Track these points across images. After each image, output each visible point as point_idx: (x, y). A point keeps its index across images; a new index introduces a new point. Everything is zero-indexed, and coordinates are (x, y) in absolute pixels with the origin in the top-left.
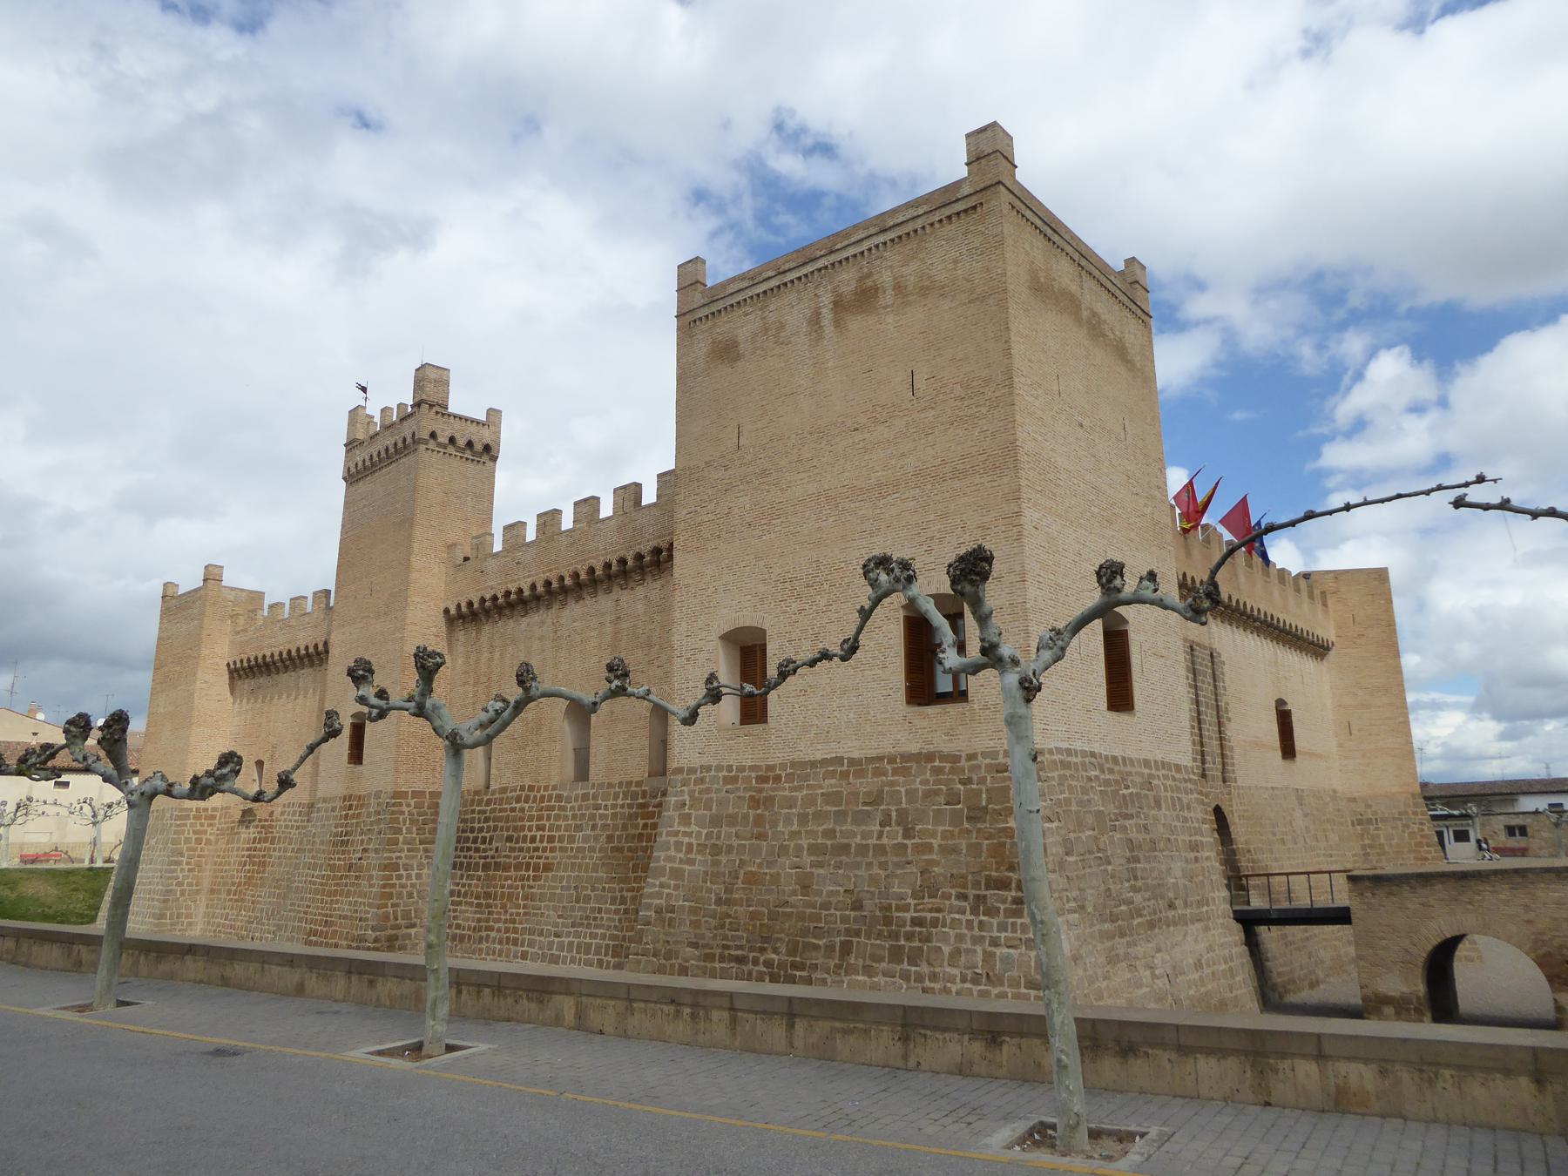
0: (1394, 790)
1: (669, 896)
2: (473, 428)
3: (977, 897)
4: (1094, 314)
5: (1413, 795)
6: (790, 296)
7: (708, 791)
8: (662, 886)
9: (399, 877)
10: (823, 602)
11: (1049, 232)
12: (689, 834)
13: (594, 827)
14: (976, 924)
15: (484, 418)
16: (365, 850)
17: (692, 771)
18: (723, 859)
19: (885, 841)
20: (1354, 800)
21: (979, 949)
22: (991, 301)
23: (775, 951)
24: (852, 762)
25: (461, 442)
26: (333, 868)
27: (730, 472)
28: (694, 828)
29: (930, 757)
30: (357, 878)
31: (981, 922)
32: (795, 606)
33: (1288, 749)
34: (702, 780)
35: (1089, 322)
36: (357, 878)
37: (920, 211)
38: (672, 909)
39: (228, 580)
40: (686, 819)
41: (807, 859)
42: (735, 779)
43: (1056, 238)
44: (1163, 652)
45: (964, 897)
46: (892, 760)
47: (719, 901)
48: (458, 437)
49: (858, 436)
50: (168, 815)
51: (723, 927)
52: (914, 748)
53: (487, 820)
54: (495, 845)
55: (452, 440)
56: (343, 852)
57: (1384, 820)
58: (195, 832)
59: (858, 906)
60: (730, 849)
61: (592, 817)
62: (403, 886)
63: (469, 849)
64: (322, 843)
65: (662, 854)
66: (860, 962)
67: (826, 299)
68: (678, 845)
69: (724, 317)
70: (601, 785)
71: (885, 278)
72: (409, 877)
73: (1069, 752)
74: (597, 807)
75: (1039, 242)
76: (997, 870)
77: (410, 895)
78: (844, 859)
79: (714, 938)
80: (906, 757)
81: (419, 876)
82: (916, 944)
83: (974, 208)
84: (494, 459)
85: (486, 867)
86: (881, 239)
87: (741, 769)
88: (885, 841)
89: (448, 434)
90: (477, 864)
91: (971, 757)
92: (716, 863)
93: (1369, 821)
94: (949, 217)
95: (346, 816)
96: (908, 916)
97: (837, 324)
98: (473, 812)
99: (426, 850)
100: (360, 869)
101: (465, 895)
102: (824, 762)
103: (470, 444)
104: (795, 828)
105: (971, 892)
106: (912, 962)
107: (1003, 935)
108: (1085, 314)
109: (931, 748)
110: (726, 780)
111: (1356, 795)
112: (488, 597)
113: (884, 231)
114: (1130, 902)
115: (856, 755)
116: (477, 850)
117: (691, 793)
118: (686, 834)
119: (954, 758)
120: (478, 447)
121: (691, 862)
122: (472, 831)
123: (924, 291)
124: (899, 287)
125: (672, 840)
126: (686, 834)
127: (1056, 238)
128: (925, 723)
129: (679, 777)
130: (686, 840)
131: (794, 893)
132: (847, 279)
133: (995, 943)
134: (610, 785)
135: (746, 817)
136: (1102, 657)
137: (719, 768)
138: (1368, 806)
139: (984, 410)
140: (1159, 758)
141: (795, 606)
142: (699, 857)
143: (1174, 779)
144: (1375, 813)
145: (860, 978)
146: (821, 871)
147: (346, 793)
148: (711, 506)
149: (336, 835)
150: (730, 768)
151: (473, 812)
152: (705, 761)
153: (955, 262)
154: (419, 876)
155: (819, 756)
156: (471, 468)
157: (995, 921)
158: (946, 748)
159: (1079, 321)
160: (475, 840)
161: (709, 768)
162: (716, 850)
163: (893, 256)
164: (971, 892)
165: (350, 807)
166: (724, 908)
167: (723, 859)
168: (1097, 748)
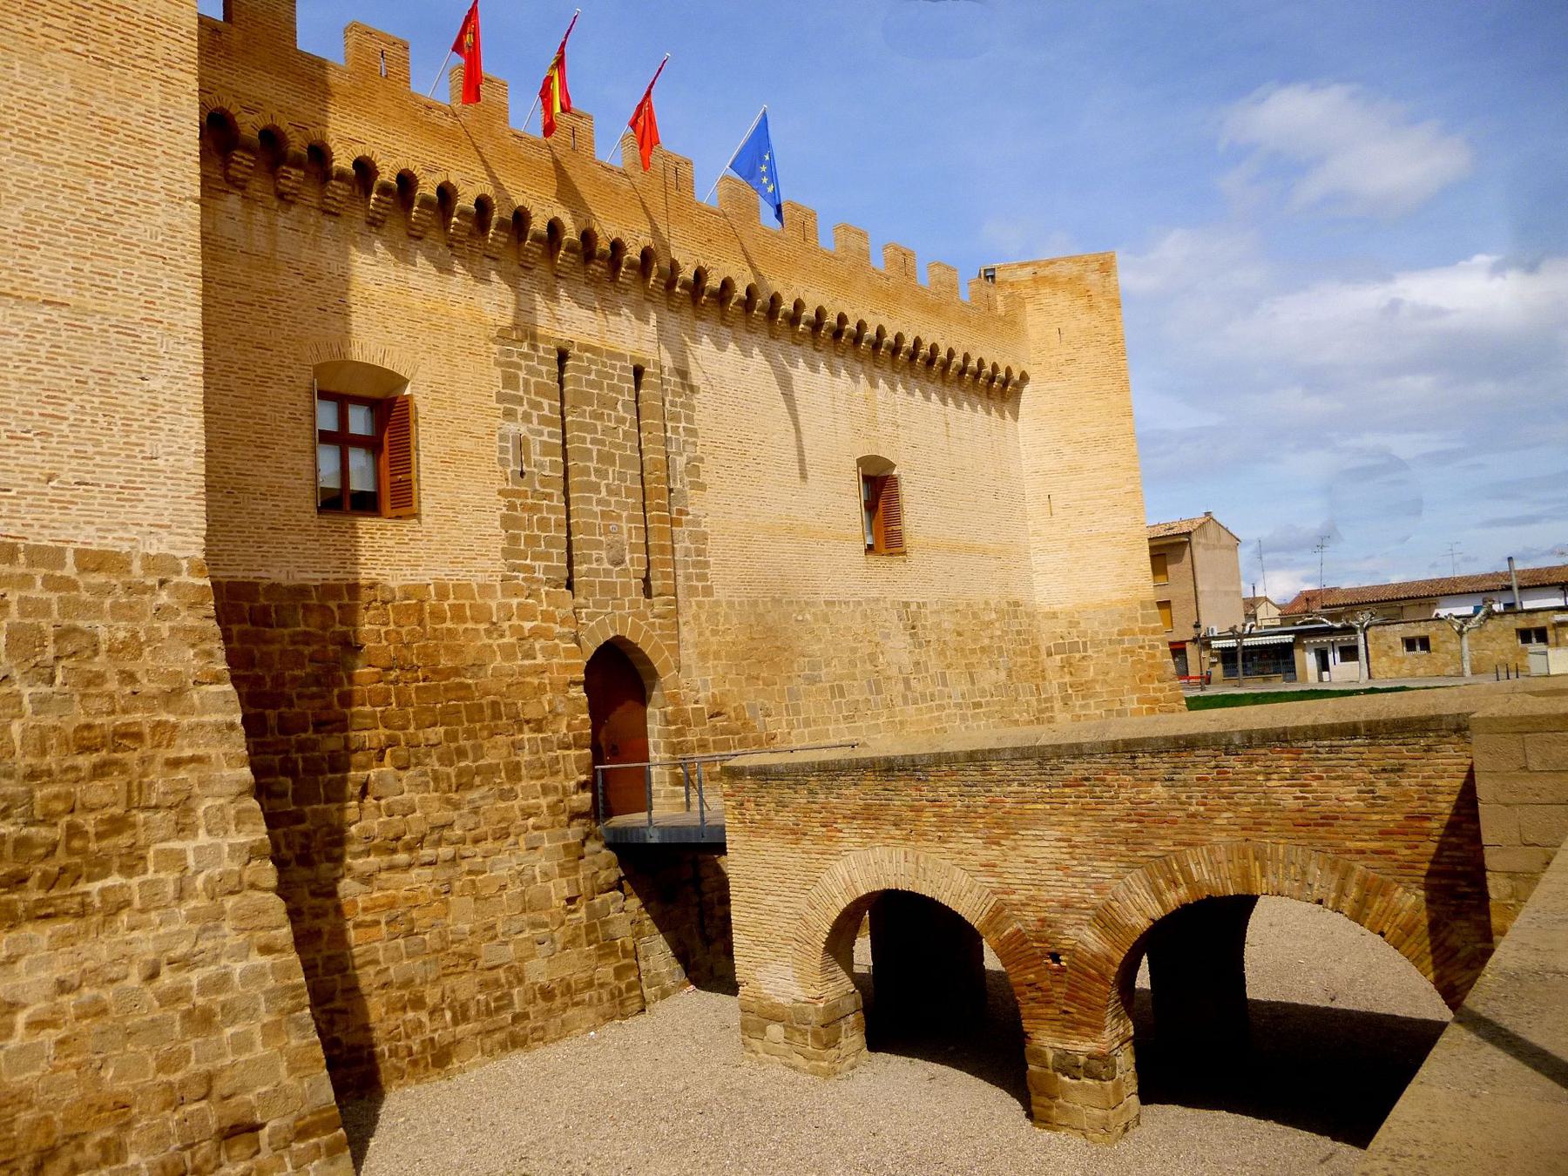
0: (1115, 596)
5: (1143, 605)
20: (1054, 615)
44: (68, 295)
57: (1097, 644)
93: (1073, 647)
111: (1057, 607)
138: (1073, 624)
144: (1085, 634)
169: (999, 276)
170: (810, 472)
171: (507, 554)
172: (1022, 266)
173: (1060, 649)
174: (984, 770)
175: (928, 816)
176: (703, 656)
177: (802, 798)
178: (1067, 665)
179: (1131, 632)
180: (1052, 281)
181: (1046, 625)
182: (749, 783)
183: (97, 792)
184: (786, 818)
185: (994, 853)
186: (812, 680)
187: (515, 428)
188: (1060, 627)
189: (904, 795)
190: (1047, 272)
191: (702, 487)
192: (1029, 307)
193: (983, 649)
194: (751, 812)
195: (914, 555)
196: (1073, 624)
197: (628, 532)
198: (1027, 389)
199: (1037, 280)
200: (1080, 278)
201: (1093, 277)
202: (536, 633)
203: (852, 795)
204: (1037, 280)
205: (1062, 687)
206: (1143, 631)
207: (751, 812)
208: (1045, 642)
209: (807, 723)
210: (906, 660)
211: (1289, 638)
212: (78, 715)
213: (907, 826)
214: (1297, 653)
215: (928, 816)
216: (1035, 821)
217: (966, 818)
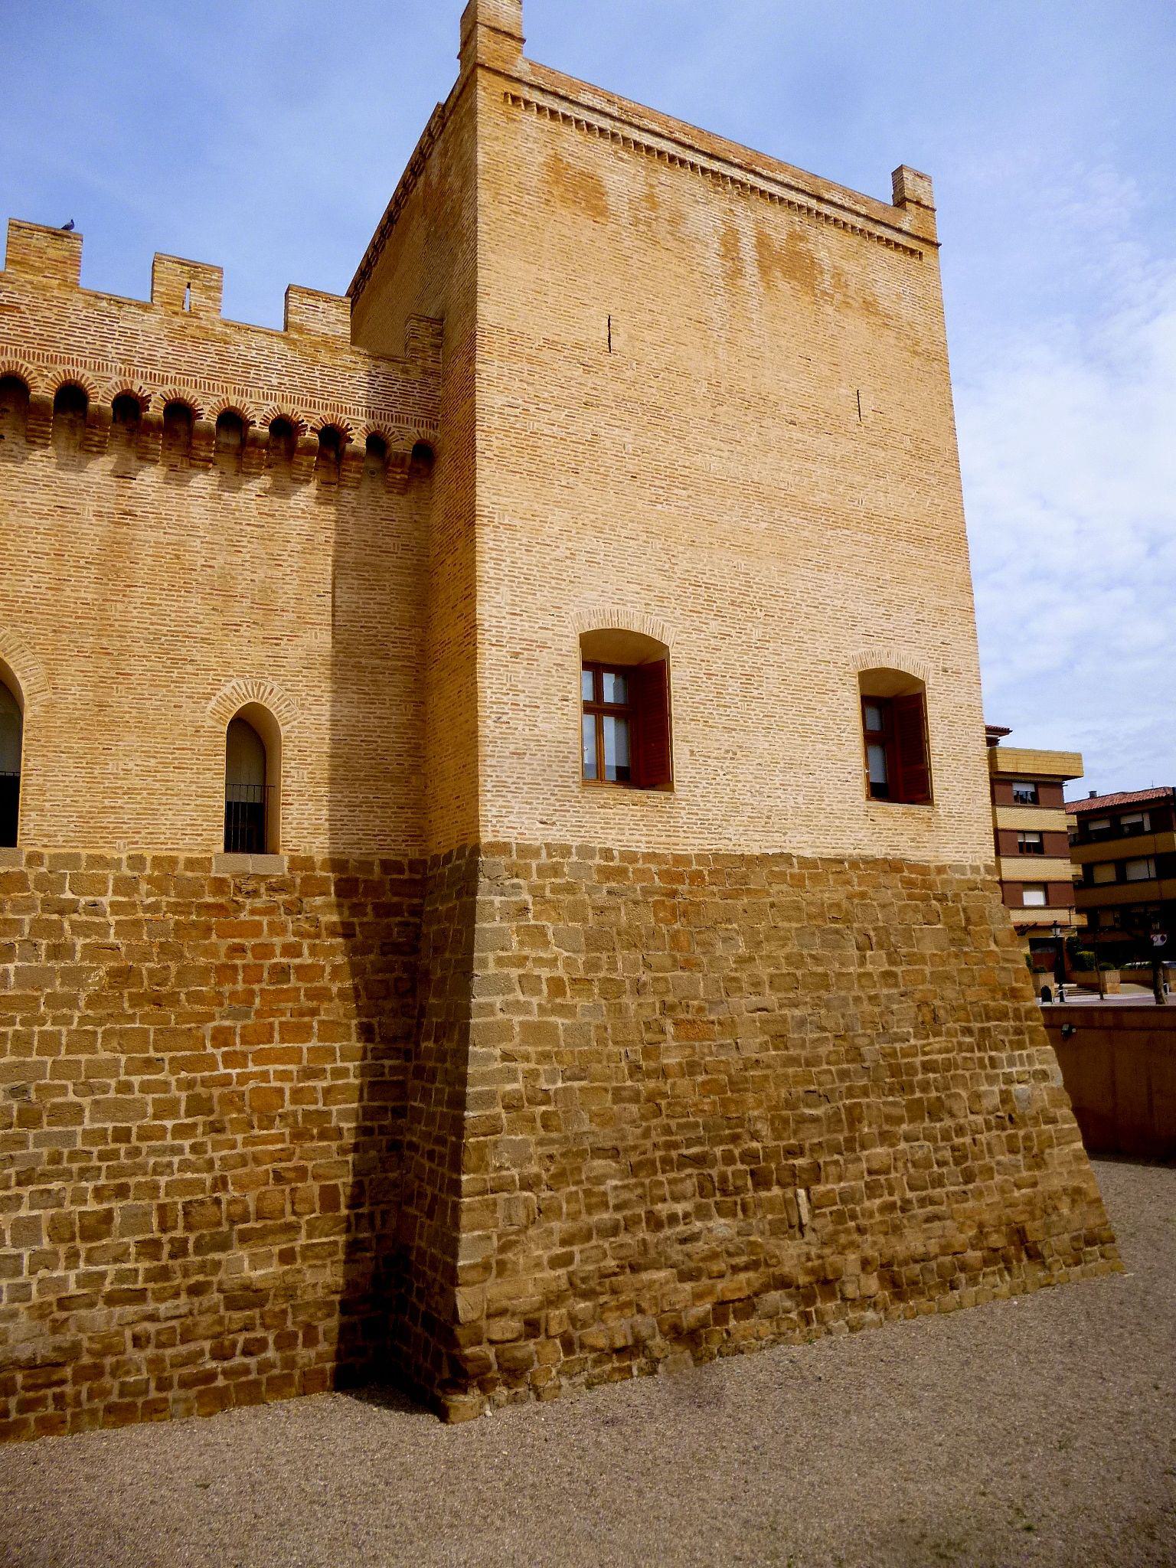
1: (532, 1075)
3: (982, 1030)
7: (570, 889)
10: (757, 634)
12: (552, 963)
14: (987, 1061)
17: (526, 851)
18: (628, 1001)
19: (869, 968)
21: (996, 1089)
23: (755, 1136)
24: (804, 862)
31: (991, 1058)
42: (622, 872)
45: (968, 1031)
46: (854, 864)
47: (635, 1069)
49: (796, 434)
51: (658, 1112)
52: (878, 851)
59: (855, 1054)
60: (639, 989)
65: (498, 1001)
66: (875, 1130)
76: (994, 999)
79: (646, 1135)
80: (871, 862)
82: (934, 1094)
87: (630, 857)
91: (941, 870)
92: (619, 1010)
96: (918, 1060)
102: (763, 859)
104: (743, 950)
106: (934, 1116)
107: (1014, 1070)
110: (607, 874)
115: (808, 853)
117: (537, 892)
118: (539, 961)
119: (923, 870)
121: (566, 1010)
125: (515, 973)
126: (539, 961)
128: (890, 824)
130: (545, 973)
131: (764, 1047)
133: (1009, 1080)
135: (653, 934)
142: (581, 1002)
145: (879, 1150)
146: (797, 1012)
150: (607, 854)
155: (757, 852)
157: (1004, 1055)
158: (914, 855)
161: (565, 851)
162: (612, 989)
166: (651, 1084)
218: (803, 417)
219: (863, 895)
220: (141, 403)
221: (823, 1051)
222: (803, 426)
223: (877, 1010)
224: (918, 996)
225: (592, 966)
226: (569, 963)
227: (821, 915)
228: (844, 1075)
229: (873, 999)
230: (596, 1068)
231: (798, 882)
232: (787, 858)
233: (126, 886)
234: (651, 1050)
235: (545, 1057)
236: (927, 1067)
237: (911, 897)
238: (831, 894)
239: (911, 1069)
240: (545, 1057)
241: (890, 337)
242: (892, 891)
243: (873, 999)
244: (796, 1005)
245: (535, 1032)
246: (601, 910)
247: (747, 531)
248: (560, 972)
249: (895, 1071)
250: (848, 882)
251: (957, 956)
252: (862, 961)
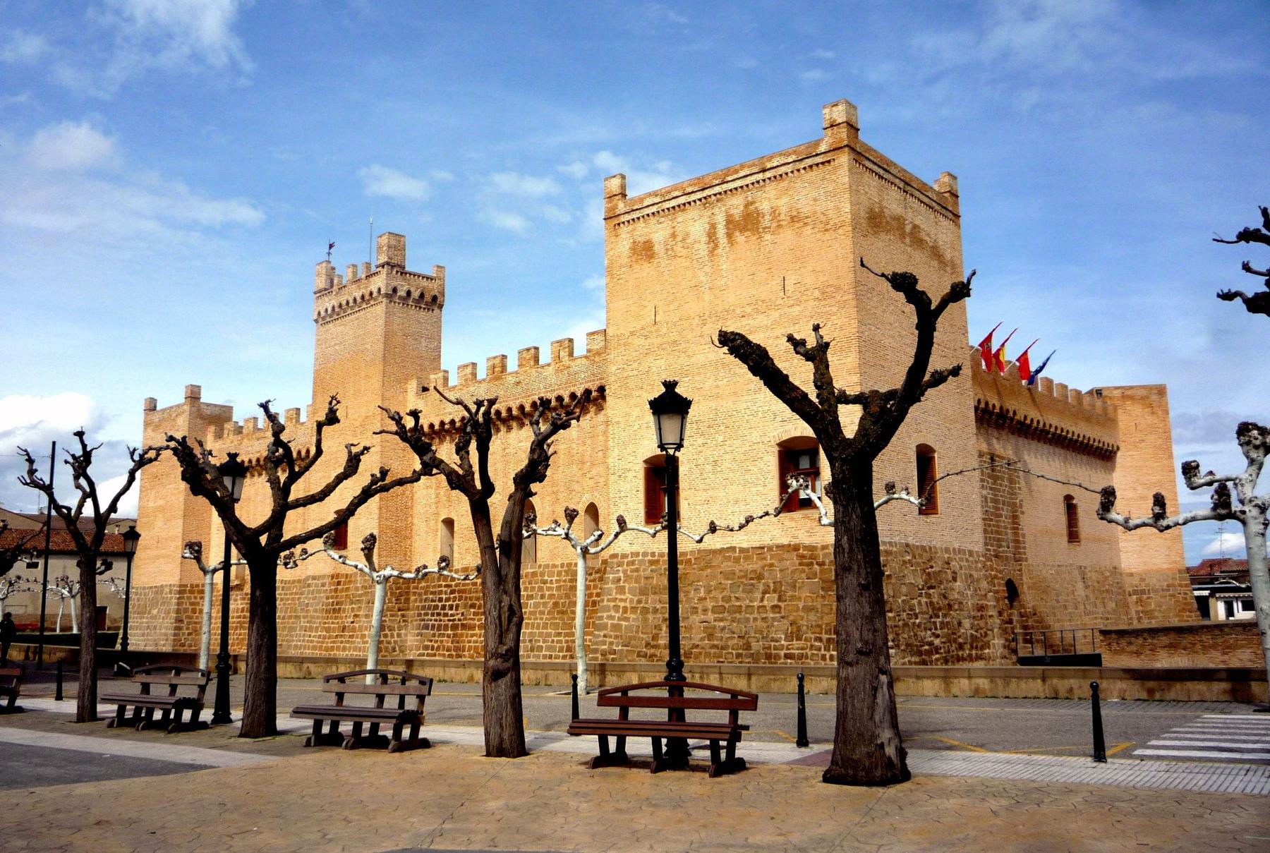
0: (1165, 566)
1: (611, 643)
2: (424, 283)
4: (915, 227)
5: (1180, 571)
6: (692, 212)
7: (637, 570)
8: (605, 636)
9: (386, 636)
10: (721, 438)
11: (882, 172)
12: (625, 600)
13: (543, 597)
15: (431, 272)
16: (356, 616)
17: (625, 556)
18: (650, 617)
19: (765, 603)
20: (1131, 575)
22: (841, 231)
24: (742, 550)
25: (416, 294)
26: (328, 630)
27: (649, 341)
28: (628, 596)
29: (796, 548)
30: (351, 637)
32: (700, 441)
33: (1073, 536)
34: (633, 563)
35: (911, 233)
36: (351, 637)
37: (790, 160)
38: (614, 652)
39: (205, 398)
40: (621, 590)
41: (710, 616)
42: (658, 561)
43: (886, 176)
45: (820, 640)
46: (770, 548)
47: (648, 645)
48: (412, 290)
50: (167, 590)
52: (785, 541)
53: (452, 592)
54: (460, 611)
55: (409, 293)
56: (336, 618)
57: (1156, 591)
58: (192, 604)
59: (748, 647)
61: (541, 589)
62: (389, 643)
63: (439, 614)
64: (316, 611)
65: (605, 615)
67: (720, 219)
68: (616, 608)
69: (641, 224)
70: (547, 566)
71: (765, 206)
72: (392, 636)
73: (890, 543)
74: (545, 582)
75: (875, 181)
77: (394, 650)
78: (738, 616)
81: (399, 635)
83: (829, 162)
84: (441, 307)
85: (454, 627)
86: (760, 176)
88: (765, 603)
89: (406, 288)
90: (446, 626)
92: (646, 620)
93: (1143, 592)
94: (811, 167)
95: (336, 590)
96: (782, 653)
97: (729, 235)
98: (440, 586)
99: (403, 616)
100: (354, 630)
101: (438, 648)
102: (722, 551)
103: (422, 296)
104: (702, 594)
105: (825, 637)
108: (908, 228)
109: (797, 541)
110: (652, 563)
112: (447, 420)
113: (764, 171)
114: (931, 644)
115: (745, 545)
116: (446, 615)
117: (625, 572)
118: (621, 600)
119: (811, 548)
120: (428, 298)
121: (627, 619)
122: (440, 600)
123: (793, 219)
124: (774, 212)
126: (621, 600)
127: (886, 176)
128: (793, 524)
129: (615, 560)
130: (622, 604)
131: (702, 639)
132: (736, 204)
134: (554, 566)
136: (916, 478)
137: (645, 554)
138: (1143, 580)
139: (834, 309)
140: (956, 546)
141: (700, 441)
142: (633, 616)
143: (967, 561)
144: (1148, 585)
147: (332, 572)
148: (635, 365)
149: (328, 604)
150: (653, 554)
151: (440, 586)
152: (635, 548)
153: (815, 200)
154: (399, 635)
155: (718, 546)
156: (423, 315)
158: (807, 541)
159: (903, 236)
160: (444, 607)
161: (637, 554)
162: (645, 611)
163: (771, 189)
164: (825, 637)
165: (339, 583)
166: (652, 651)
167: (650, 617)
168: (911, 540)
169: (1104, 393)
170: (1062, 508)
171: (986, 544)
172: (1117, 388)
173: (1135, 592)
174: (1221, 631)
175: (1198, 646)
176: (1029, 588)
177: (1140, 641)
178: (1139, 601)
179: (1173, 585)
180: (1132, 398)
181: (1127, 580)
182: (1114, 636)
183: (982, 623)
184: (1133, 648)
185: (1226, 657)
186: (1058, 601)
187: (984, 492)
188: (1136, 581)
189: (1187, 639)
190: (1129, 393)
191: (1023, 513)
192: (1120, 411)
193: (1107, 591)
194: (1114, 646)
195: (1083, 542)
196: (1143, 580)
197: (1011, 537)
198: (1119, 454)
199: (1124, 397)
200: (1147, 397)
201: (1154, 397)
202: (996, 577)
203: (1165, 640)
204: (1124, 397)
205: (1137, 612)
206: (1181, 586)
207: (1114, 646)
208: (1129, 589)
209: (1058, 621)
210: (1083, 593)
211: (1206, 593)
212: (975, 601)
213: (1190, 649)
214: (1212, 601)
215: (1198, 646)
216: (1242, 647)
217: (1214, 647)
218: (748, 309)
219: (771, 565)
220: (549, 401)
221: (730, 643)
222: (749, 315)
223: (765, 625)
224: (791, 618)
225: (639, 602)
226: (632, 600)
227: (745, 576)
228: (739, 655)
229: (764, 619)
230: (633, 642)
231: (737, 560)
232: (733, 549)
233: (559, 574)
234: (655, 637)
235: (617, 637)
236: (787, 656)
237: (800, 564)
238: (754, 565)
239: (777, 657)
240: (617, 637)
241: (808, 231)
242: (792, 561)
243: (764, 619)
244: (721, 620)
245: (616, 627)
246: (647, 578)
247: (718, 387)
248: (628, 604)
249: (768, 657)
250: (765, 559)
251: (823, 597)
252: (762, 600)
